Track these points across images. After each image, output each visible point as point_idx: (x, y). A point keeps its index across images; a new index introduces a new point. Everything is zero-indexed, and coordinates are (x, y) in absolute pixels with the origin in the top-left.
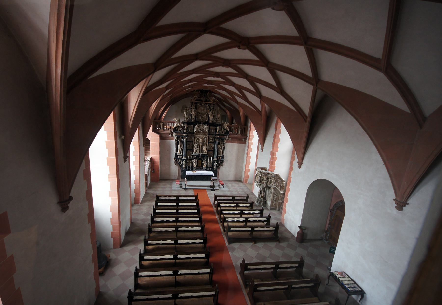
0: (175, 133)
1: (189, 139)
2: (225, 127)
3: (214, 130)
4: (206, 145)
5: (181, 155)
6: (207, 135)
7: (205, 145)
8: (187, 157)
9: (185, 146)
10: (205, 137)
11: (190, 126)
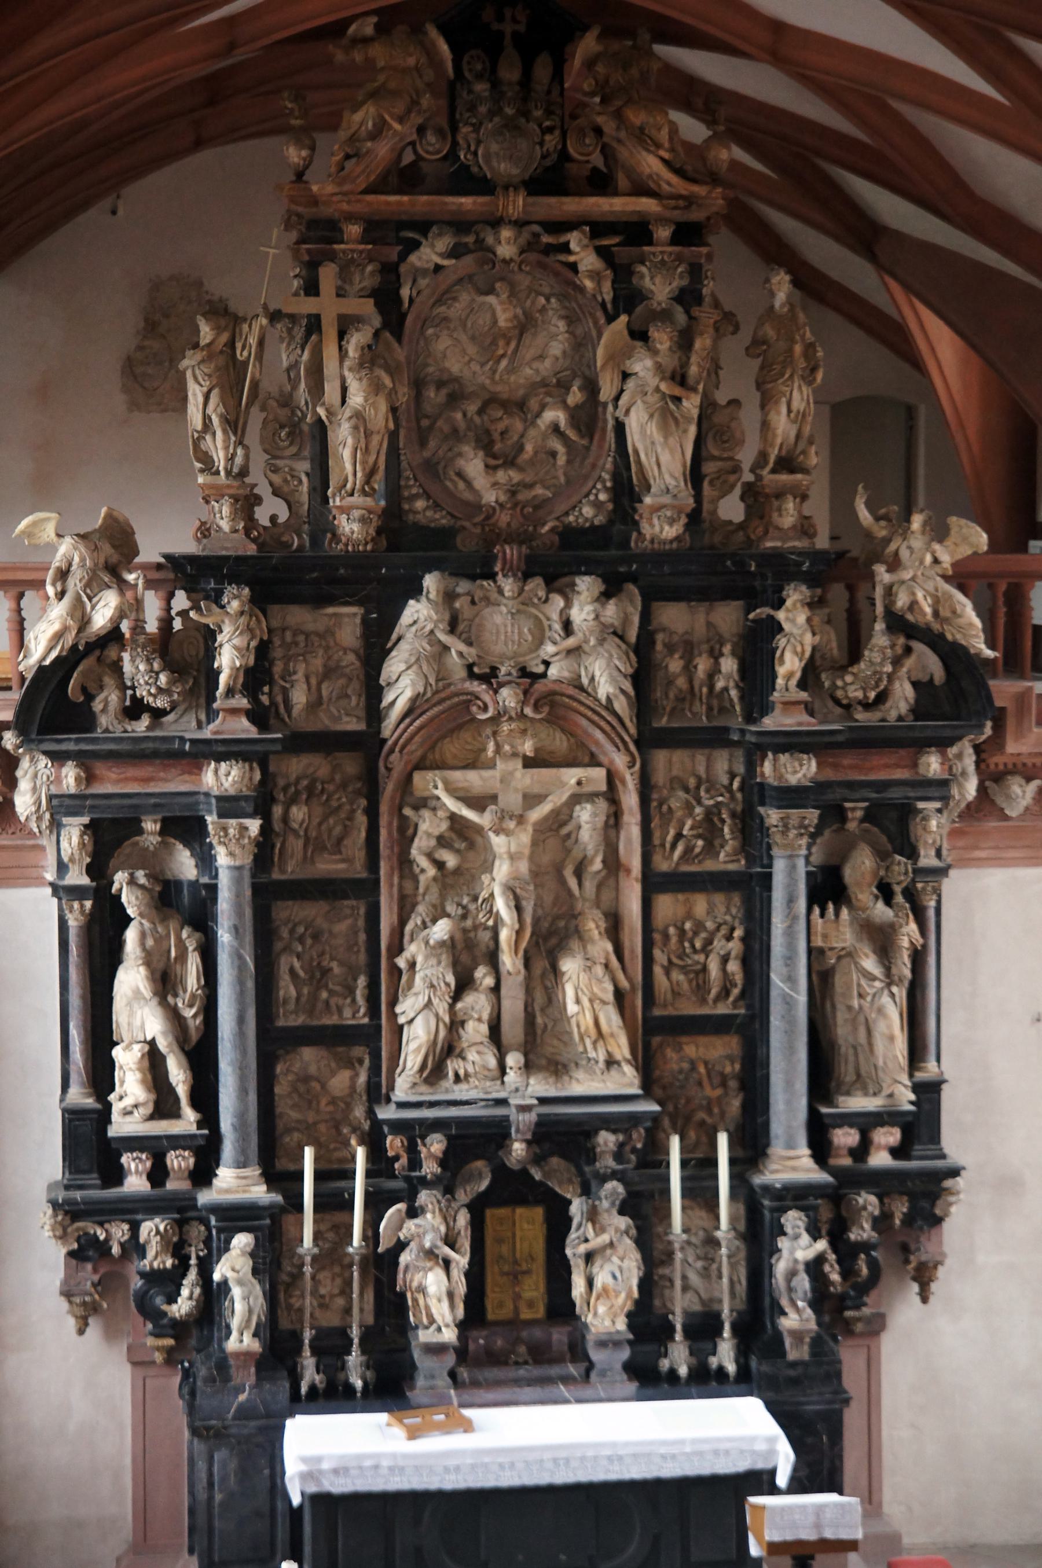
0: (58, 758)
1: (296, 845)
2: (913, 605)
3: (729, 665)
4: (614, 928)
5: (177, 1142)
6: (620, 761)
7: (593, 925)
8: (283, 1164)
9: (240, 981)
10: (576, 799)
11: (299, 616)
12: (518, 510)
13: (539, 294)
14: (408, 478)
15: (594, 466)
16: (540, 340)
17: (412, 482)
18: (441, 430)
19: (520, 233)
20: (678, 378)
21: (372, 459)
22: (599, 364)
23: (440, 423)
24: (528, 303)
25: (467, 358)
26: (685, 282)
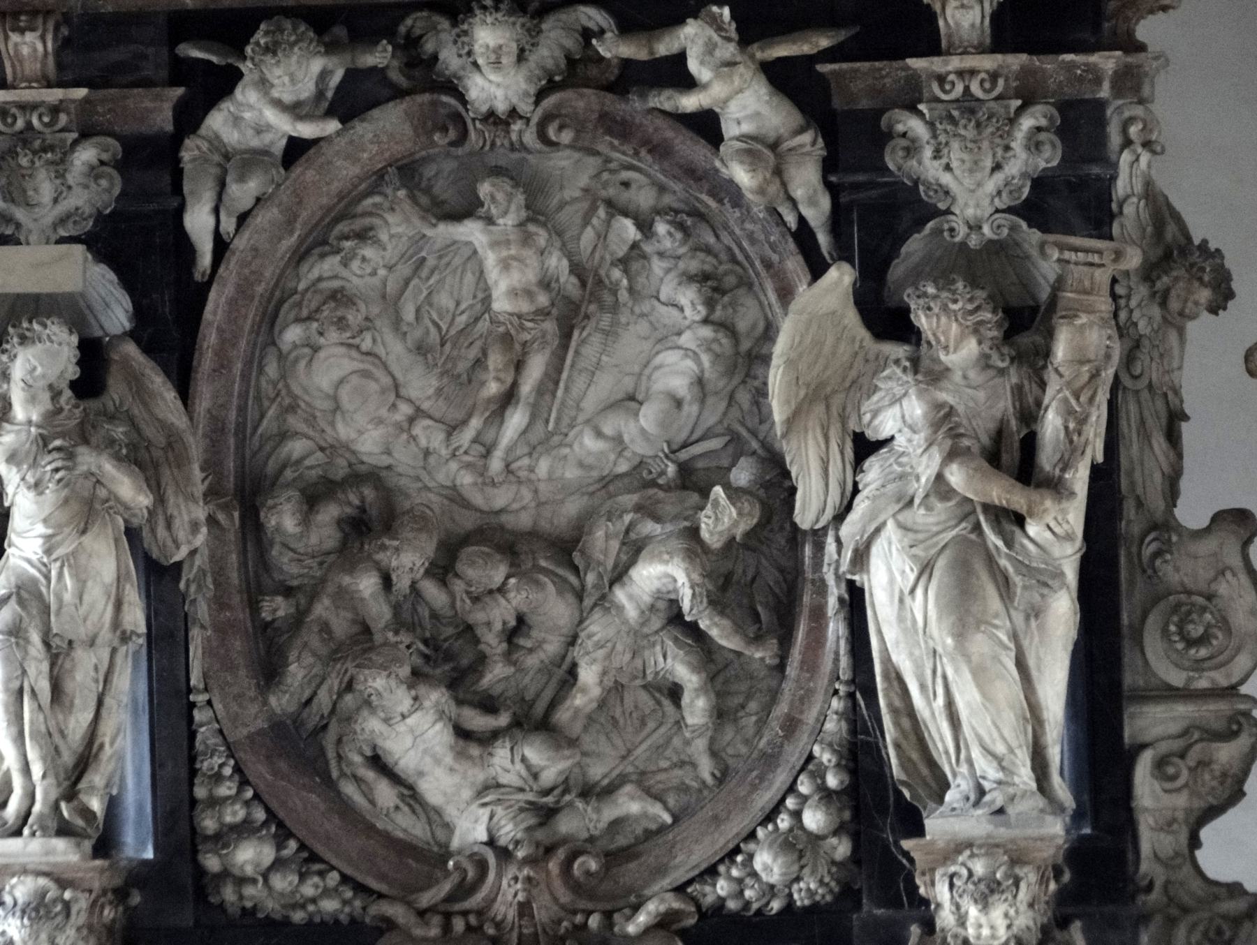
12: (553, 866)
13: (616, 208)
14: (218, 778)
15: (791, 725)
16: (632, 343)
17: (225, 790)
18: (325, 628)
19: (534, 33)
20: (1011, 455)
21: (79, 721)
22: (778, 413)
23: (322, 608)
24: (589, 235)
25: (405, 409)
26: (1049, 158)
